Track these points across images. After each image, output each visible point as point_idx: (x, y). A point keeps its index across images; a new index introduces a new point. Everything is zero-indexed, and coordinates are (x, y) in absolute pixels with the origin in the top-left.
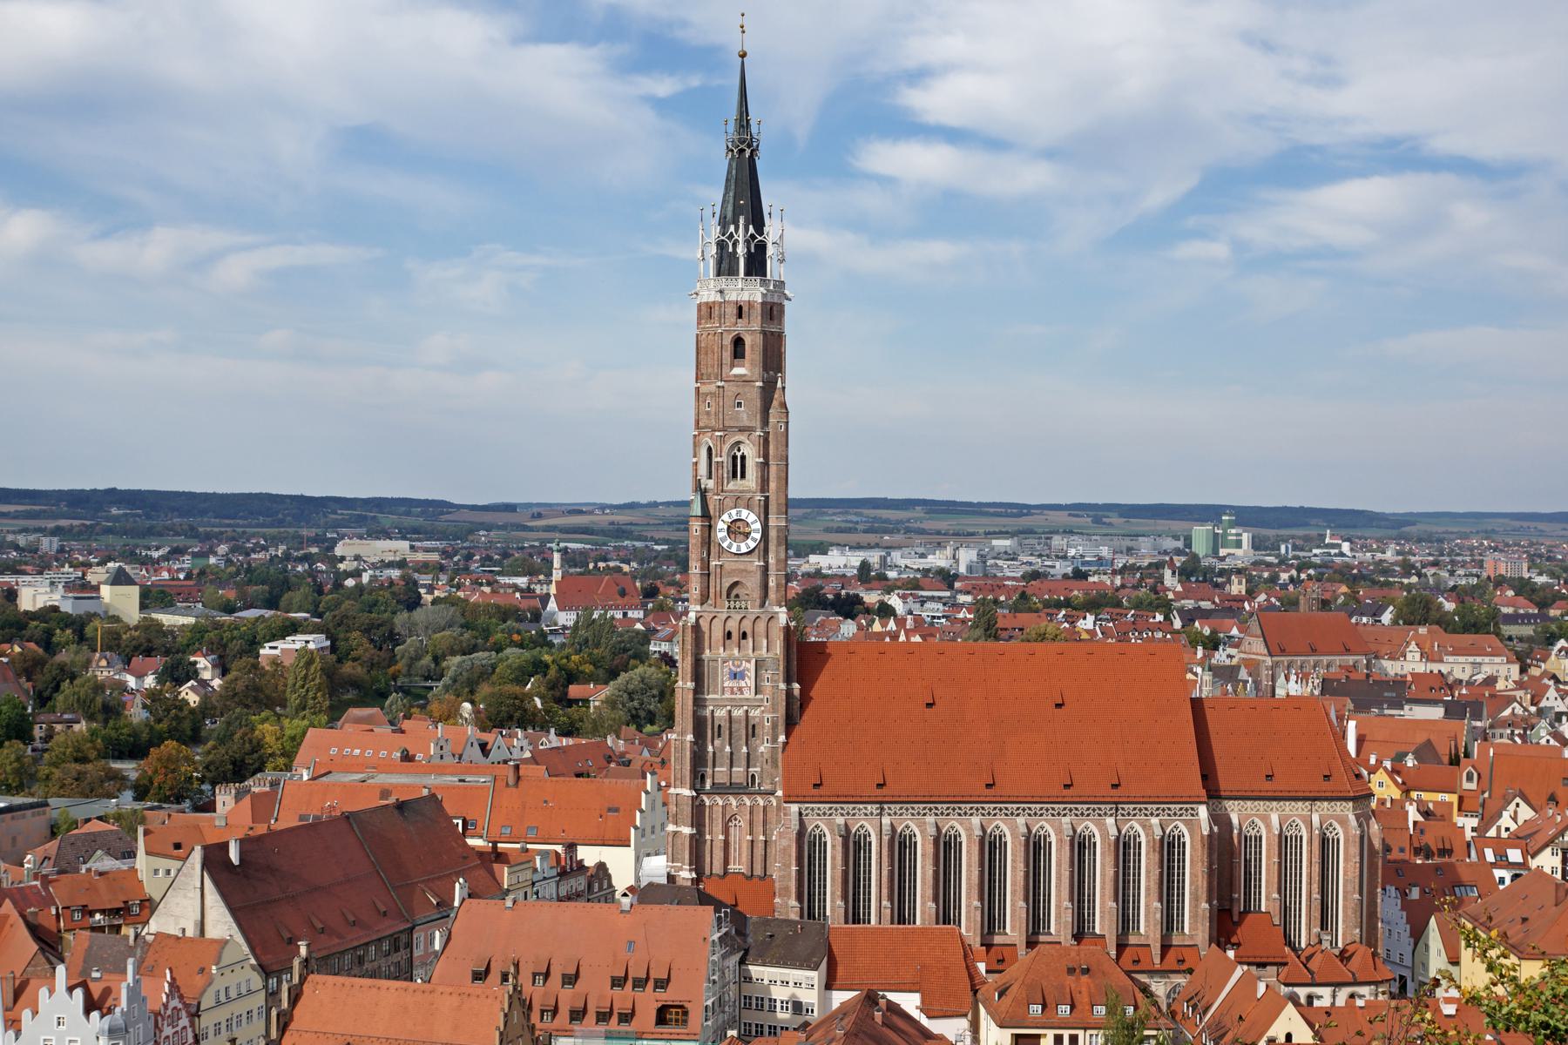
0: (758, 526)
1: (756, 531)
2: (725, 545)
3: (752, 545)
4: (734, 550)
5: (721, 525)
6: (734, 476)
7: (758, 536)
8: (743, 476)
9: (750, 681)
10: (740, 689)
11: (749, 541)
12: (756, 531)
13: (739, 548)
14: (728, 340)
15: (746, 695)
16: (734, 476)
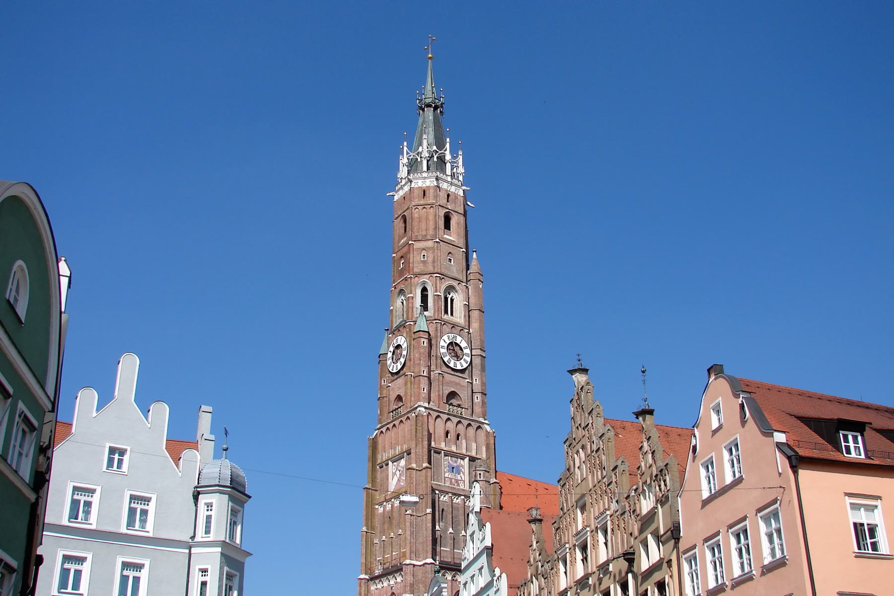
0: (467, 351)
1: (467, 355)
2: (446, 359)
3: (465, 365)
4: (452, 365)
5: (442, 343)
6: (446, 312)
7: (469, 359)
8: (452, 314)
9: (465, 476)
10: (457, 481)
11: (462, 361)
12: (467, 355)
13: (455, 365)
14: (442, 212)
15: (462, 487)
16: (446, 312)
